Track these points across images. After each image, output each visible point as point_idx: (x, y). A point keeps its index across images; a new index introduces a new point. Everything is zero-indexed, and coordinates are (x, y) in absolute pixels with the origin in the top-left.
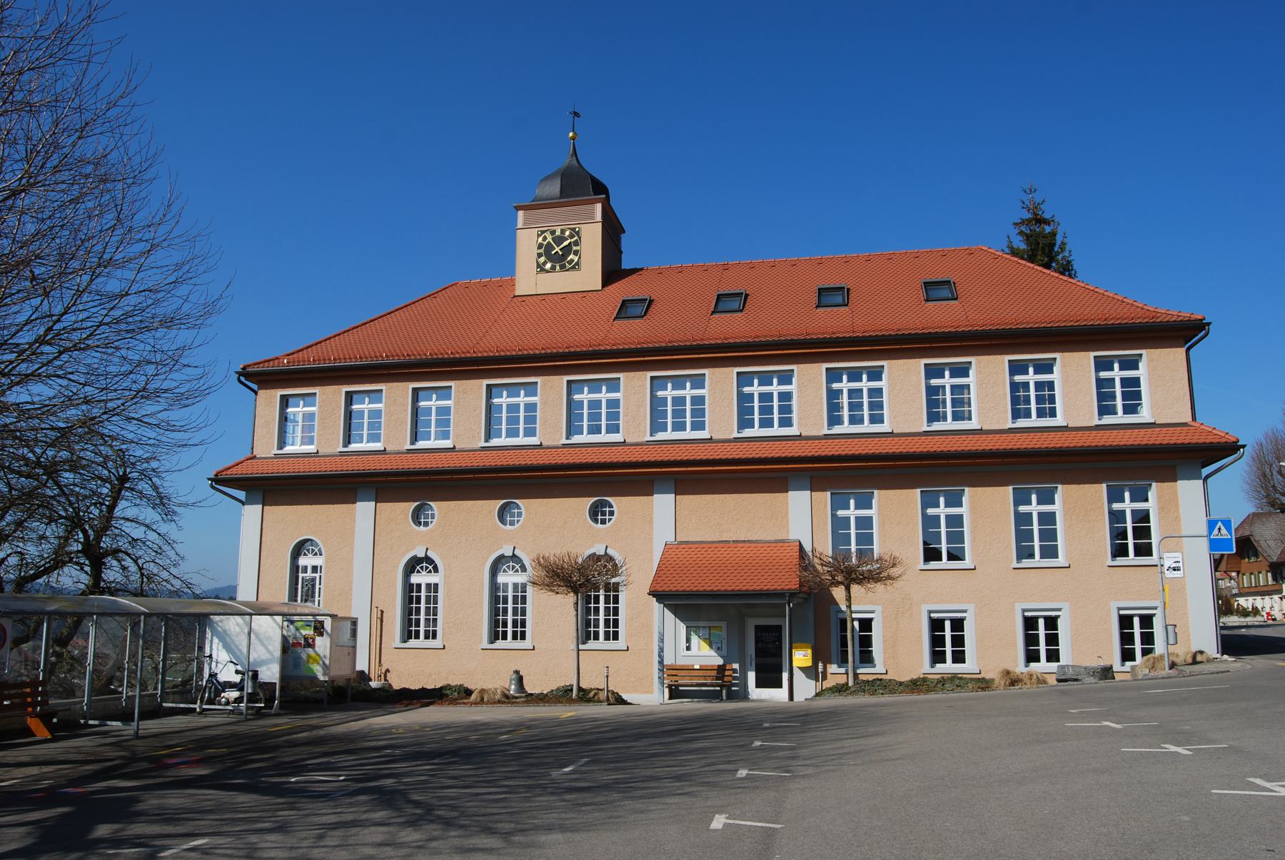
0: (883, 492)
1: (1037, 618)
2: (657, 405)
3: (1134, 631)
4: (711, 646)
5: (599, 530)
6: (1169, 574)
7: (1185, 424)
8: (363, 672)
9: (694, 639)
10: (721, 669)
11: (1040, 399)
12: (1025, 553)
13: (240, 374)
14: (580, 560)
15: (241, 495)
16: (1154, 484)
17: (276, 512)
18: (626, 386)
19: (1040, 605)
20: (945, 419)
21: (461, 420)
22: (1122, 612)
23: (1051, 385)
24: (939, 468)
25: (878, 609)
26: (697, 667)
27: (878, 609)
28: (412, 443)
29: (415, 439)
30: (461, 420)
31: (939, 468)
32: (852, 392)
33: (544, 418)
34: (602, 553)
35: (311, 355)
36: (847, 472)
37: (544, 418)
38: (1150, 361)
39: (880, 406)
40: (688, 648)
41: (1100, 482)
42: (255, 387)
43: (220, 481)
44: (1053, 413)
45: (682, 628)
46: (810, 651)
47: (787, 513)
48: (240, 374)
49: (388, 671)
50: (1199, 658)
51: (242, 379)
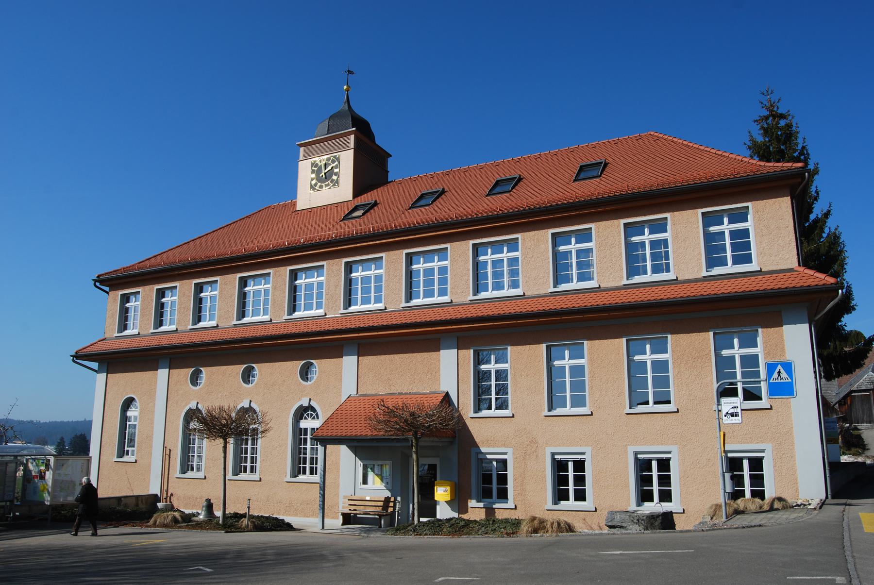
0: (515, 347)
1: (567, 462)
2: (633, 254)
3: (743, 473)
4: (382, 480)
5: (305, 386)
6: (727, 420)
7: (791, 270)
8: (156, 495)
9: (371, 475)
10: (387, 500)
11: (654, 257)
12: (637, 399)
13: (95, 281)
14: (233, 415)
15: (95, 365)
16: (760, 330)
17: (115, 377)
18: (328, 271)
19: (652, 448)
20: (645, 273)
21: (267, 301)
22: (730, 455)
23: (745, 233)
24: (560, 324)
25: (510, 451)
26: (368, 498)
27: (510, 451)
28: (407, 301)
29: (476, 291)
30: (267, 301)
31: (560, 324)
32: (495, 263)
33: (323, 295)
34: (307, 405)
35: (148, 263)
36: (483, 331)
37: (323, 295)
38: (756, 211)
39: (589, 265)
40: (365, 482)
41: (620, 336)
42: (107, 289)
43: (79, 357)
44: (748, 259)
45: (360, 464)
46: (448, 488)
47: (439, 368)
48: (95, 281)
49: (172, 495)
50: (777, 505)
51: (98, 284)
